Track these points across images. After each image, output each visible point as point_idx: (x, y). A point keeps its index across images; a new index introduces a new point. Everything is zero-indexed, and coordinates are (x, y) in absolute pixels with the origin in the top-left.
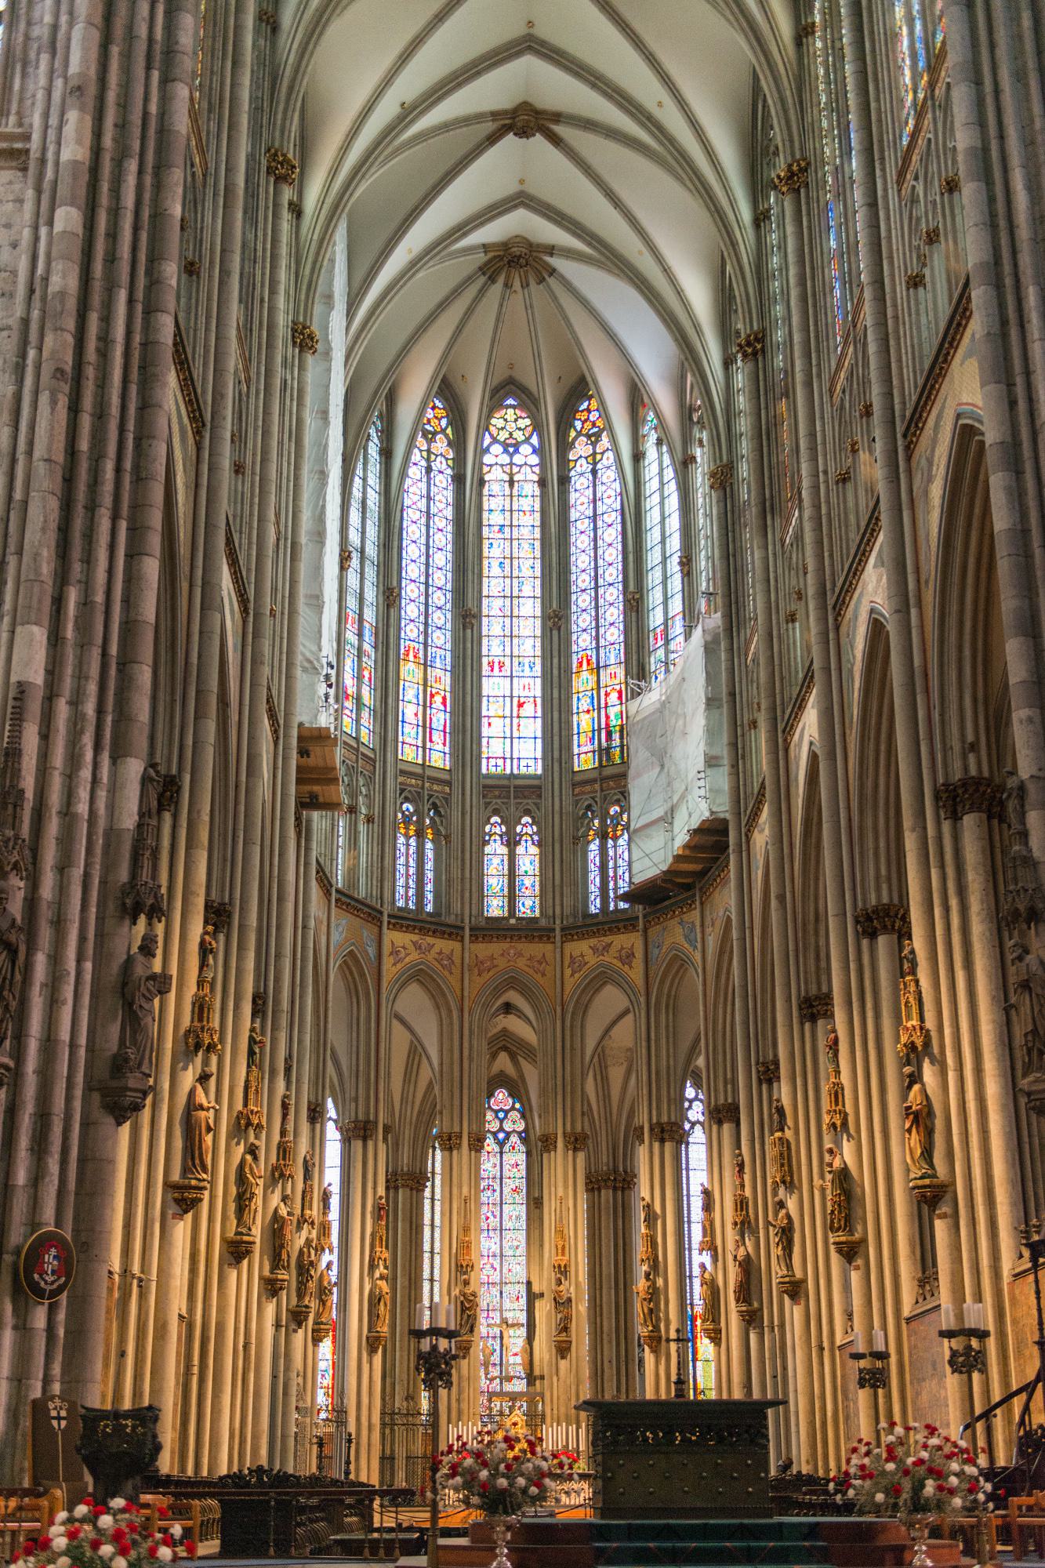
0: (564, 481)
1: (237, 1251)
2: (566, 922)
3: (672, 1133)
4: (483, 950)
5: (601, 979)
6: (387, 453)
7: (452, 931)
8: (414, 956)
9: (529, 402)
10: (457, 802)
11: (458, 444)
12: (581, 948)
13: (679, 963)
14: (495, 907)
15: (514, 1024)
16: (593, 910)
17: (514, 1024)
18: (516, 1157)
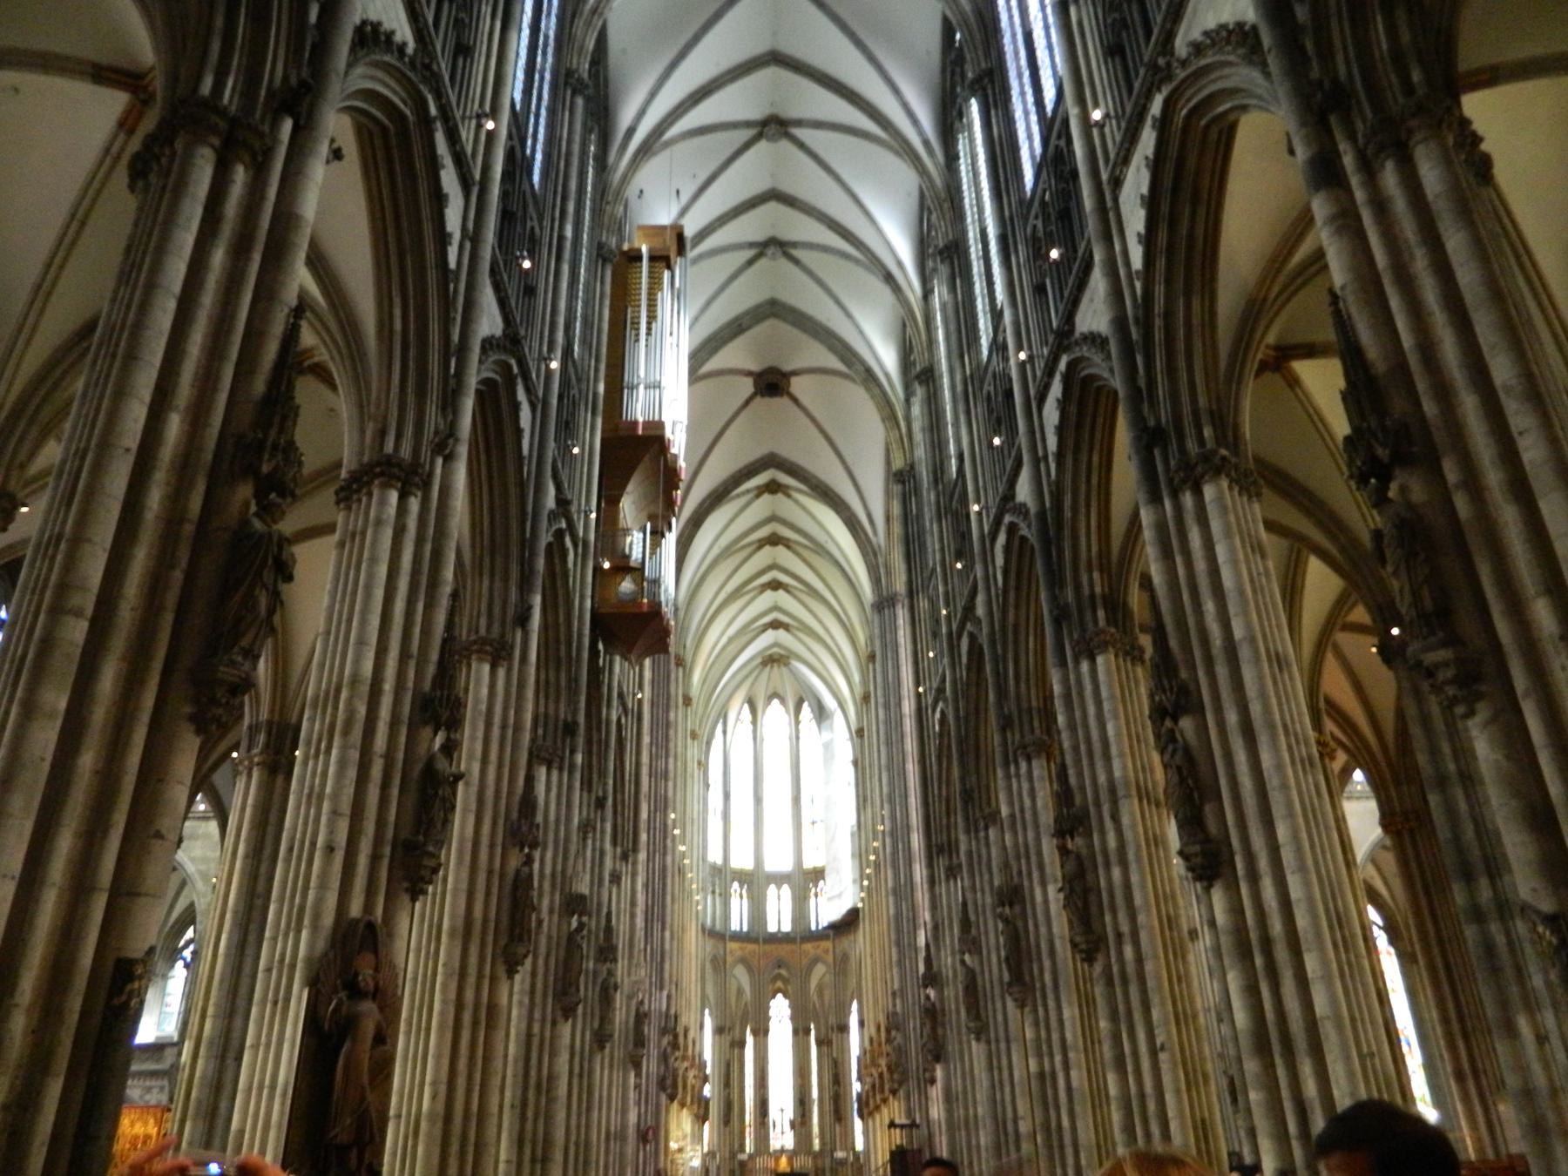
0: (798, 738)
1: (683, 1105)
2: (803, 935)
3: (843, 1028)
4: (768, 948)
5: (816, 960)
6: (725, 732)
7: (755, 941)
8: (739, 953)
9: (783, 701)
10: (756, 883)
11: (754, 722)
12: (808, 947)
13: (845, 958)
14: (772, 928)
15: (783, 972)
16: (813, 928)
17: (783, 972)
18: (788, 1027)
